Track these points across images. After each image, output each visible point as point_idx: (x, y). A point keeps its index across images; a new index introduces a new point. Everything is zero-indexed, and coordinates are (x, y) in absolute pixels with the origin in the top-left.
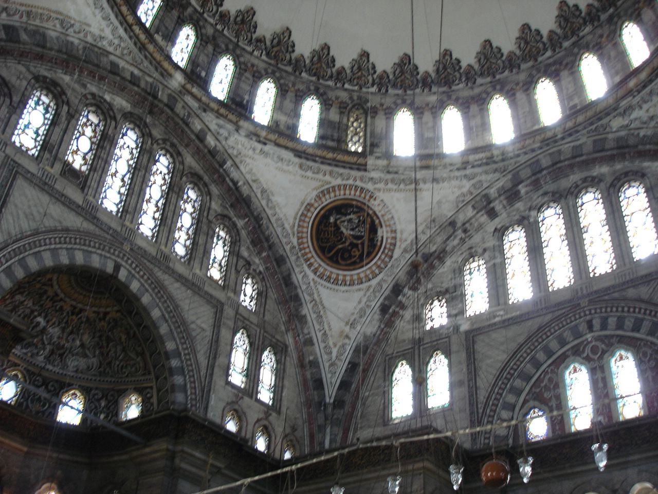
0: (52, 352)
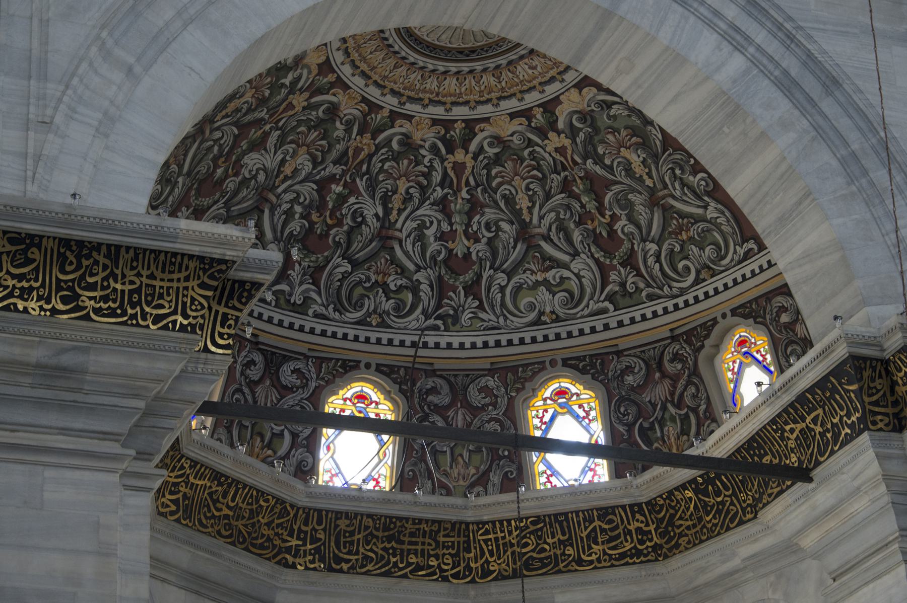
0: (441, 289)
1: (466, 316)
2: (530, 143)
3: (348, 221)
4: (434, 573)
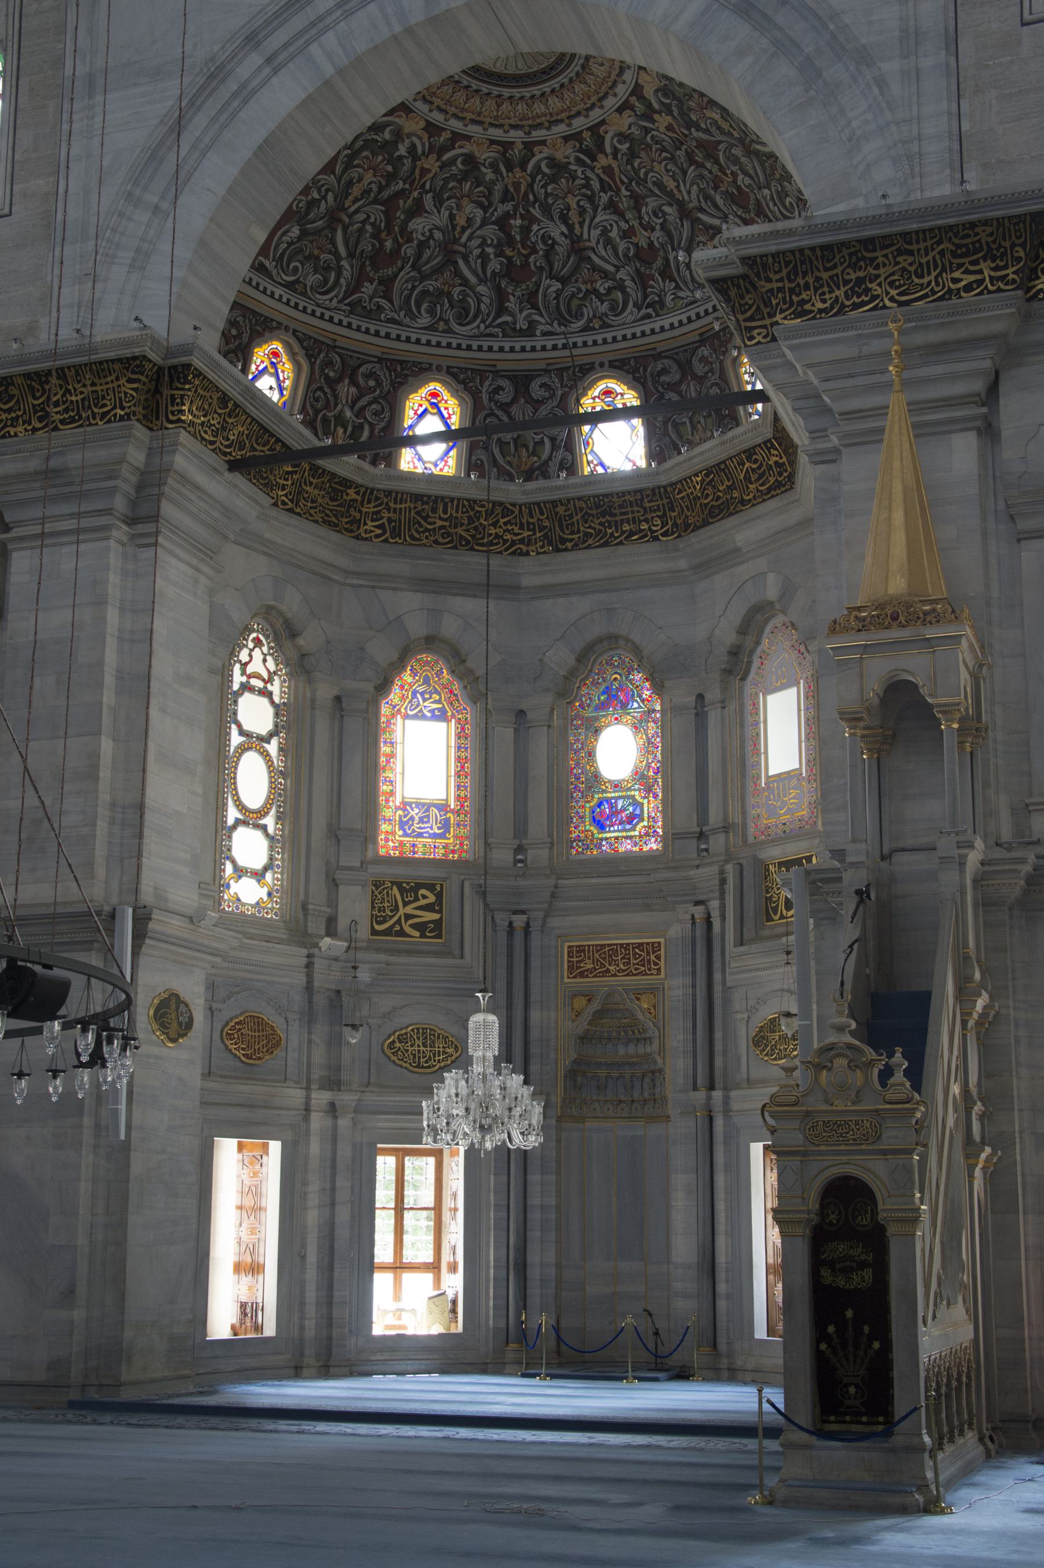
0: (642, 281)
1: (669, 298)
2: (647, 130)
3: (540, 246)
4: (646, 536)
